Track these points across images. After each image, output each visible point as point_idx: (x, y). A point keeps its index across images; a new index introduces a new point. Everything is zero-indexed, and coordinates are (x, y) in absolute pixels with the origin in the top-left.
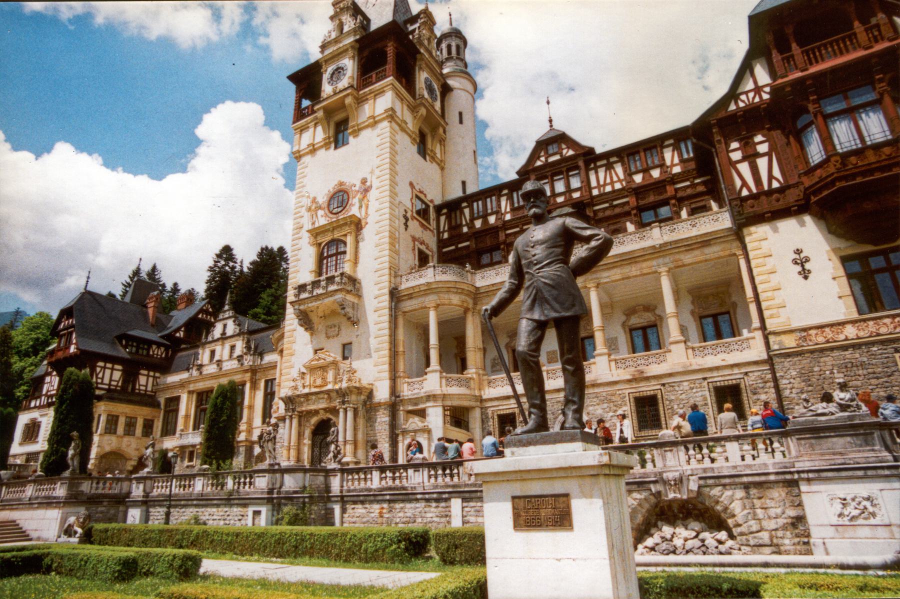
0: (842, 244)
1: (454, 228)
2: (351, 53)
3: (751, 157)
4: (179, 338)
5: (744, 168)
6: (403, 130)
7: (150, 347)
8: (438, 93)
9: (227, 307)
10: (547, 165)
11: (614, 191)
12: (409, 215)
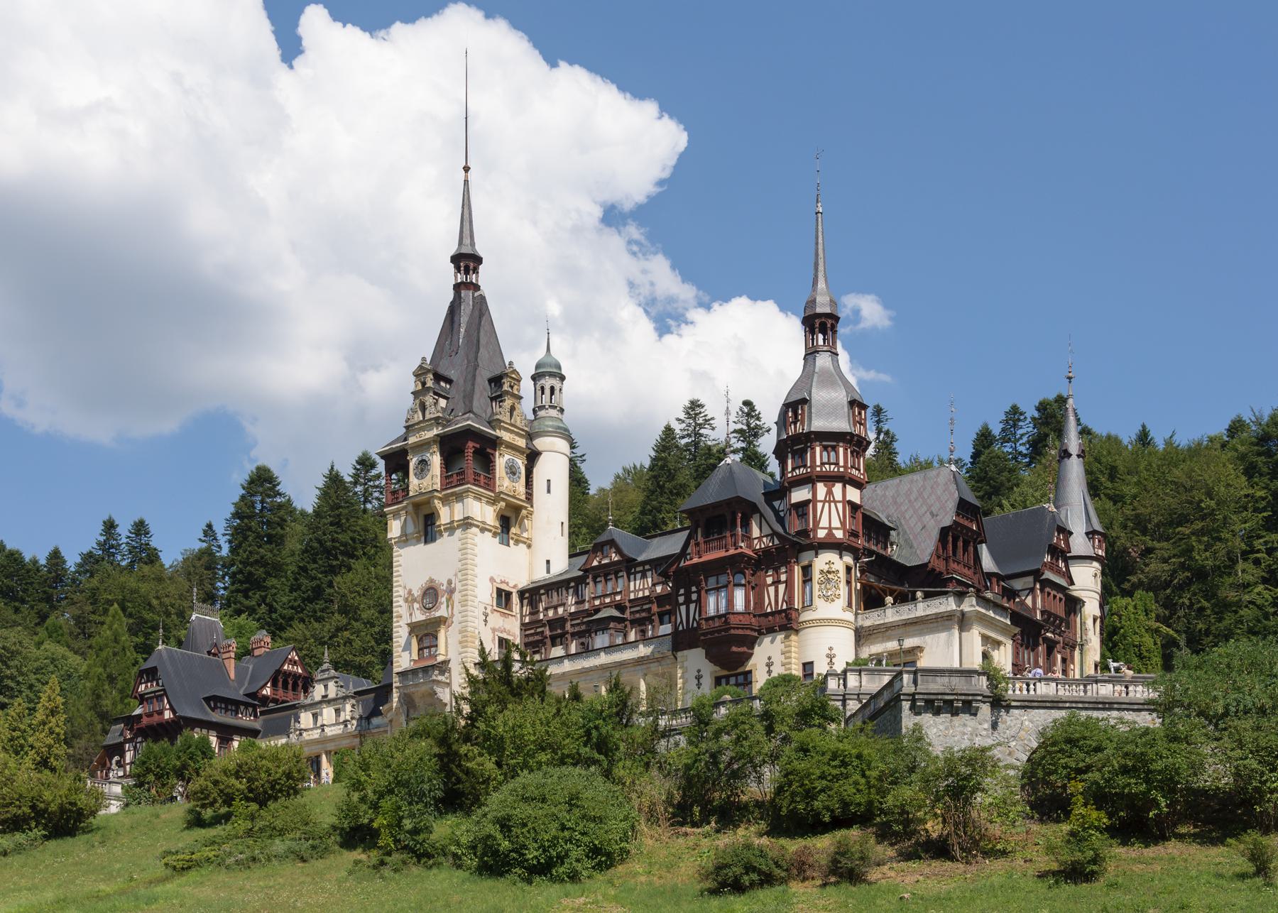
0: (718, 668)
1: (534, 612)
2: (435, 448)
3: (688, 602)
5: (683, 608)
6: (483, 530)
9: (325, 666)
10: (601, 566)
11: (644, 597)
12: (488, 611)
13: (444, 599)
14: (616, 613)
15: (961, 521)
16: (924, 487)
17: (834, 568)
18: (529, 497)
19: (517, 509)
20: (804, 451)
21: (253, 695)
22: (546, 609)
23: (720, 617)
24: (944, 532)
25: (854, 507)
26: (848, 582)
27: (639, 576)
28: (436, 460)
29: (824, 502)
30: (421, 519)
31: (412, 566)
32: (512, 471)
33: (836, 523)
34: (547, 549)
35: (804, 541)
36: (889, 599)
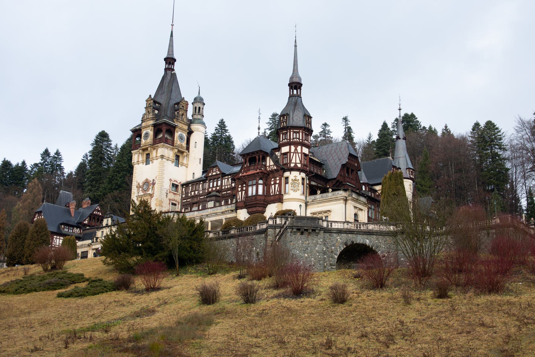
1: (187, 193)
2: (151, 128)
4: (85, 224)
6: (168, 160)
7: (73, 228)
8: (186, 138)
9: (108, 213)
10: (212, 176)
12: (168, 192)
13: (151, 187)
14: (218, 194)
15: (351, 162)
16: (337, 149)
17: (297, 178)
18: (188, 148)
19: (182, 153)
20: (287, 133)
21: (81, 223)
22: (191, 192)
23: (252, 196)
24: (343, 166)
25: (305, 155)
26: (303, 184)
27: (226, 180)
28: (151, 133)
29: (294, 153)
30: (145, 155)
31: (141, 172)
32: (181, 138)
33: (298, 161)
34: (193, 168)
35: (284, 167)
36: (319, 192)
